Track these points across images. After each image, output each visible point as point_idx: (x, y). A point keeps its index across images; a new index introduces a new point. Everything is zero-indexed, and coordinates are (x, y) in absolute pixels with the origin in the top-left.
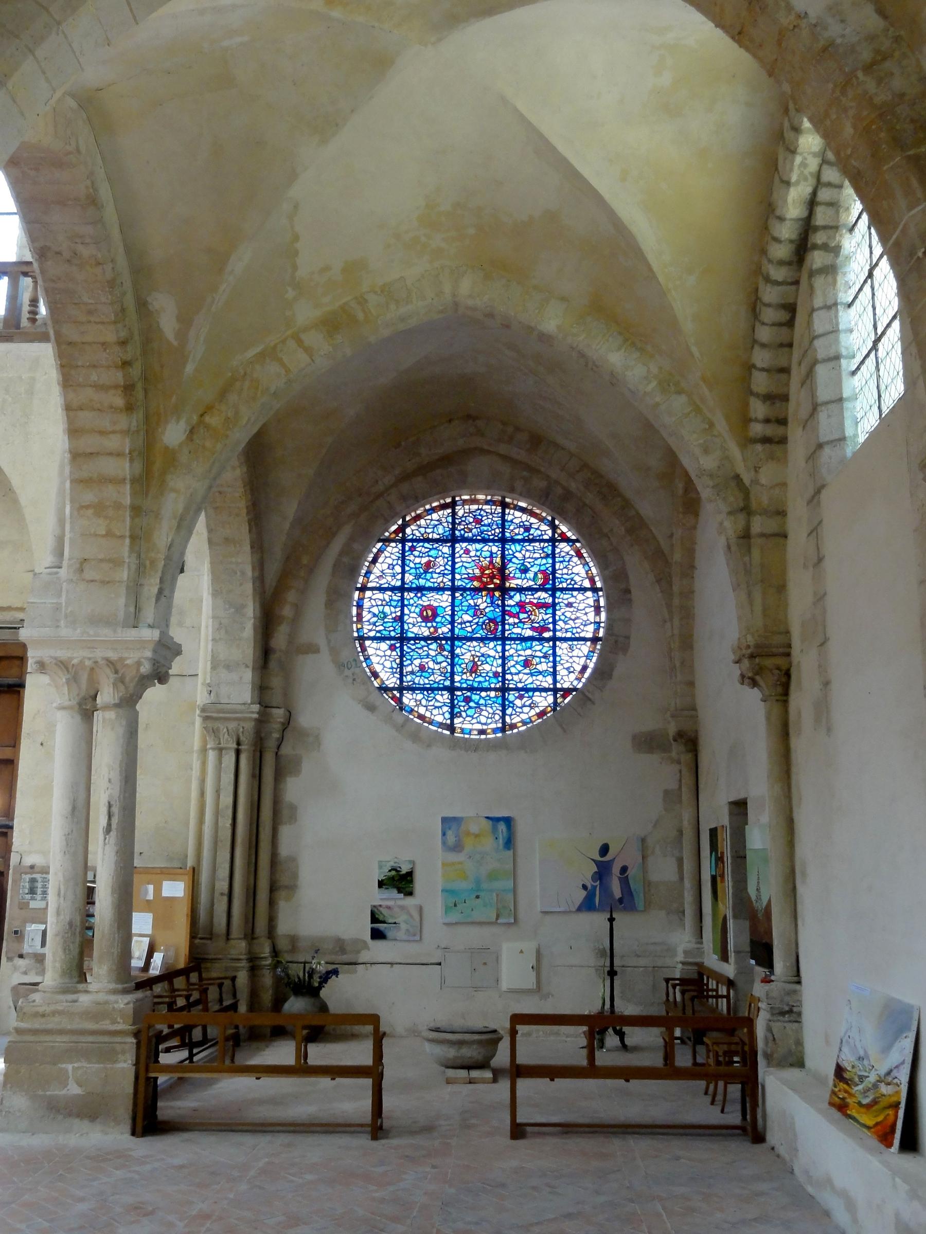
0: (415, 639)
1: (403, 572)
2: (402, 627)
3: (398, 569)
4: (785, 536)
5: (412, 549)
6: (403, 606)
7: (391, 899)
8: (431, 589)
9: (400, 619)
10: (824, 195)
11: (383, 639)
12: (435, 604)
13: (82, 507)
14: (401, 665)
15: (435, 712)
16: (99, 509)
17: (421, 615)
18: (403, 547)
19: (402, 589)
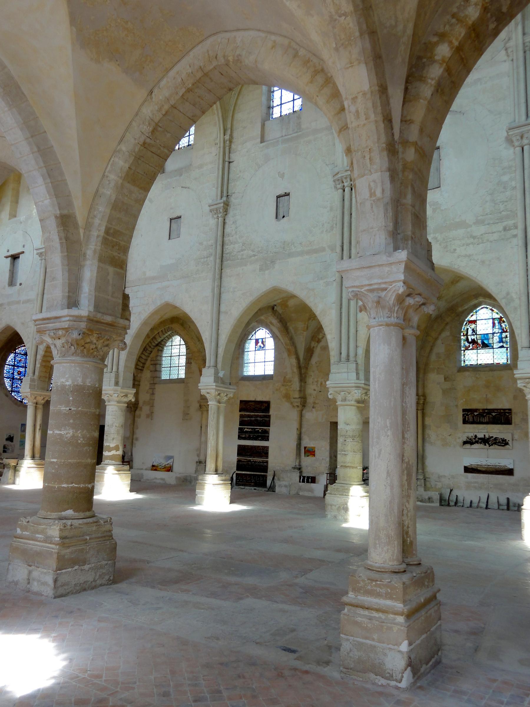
0: (16, 379)
1: (15, 361)
2: (13, 375)
3: (13, 360)
4: (140, 385)
5: (17, 356)
6: (14, 370)
7: (8, 443)
8: (21, 367)
9: (13, 373)
10: (164, 340)
11: (8, 378)
12: (21, 371)
13: (42, 366)
14: (12, 385)
15: (19, 398)
16: (45, 366)
17: (17, 373)
18: (15, 355)
19: (14, 366)
